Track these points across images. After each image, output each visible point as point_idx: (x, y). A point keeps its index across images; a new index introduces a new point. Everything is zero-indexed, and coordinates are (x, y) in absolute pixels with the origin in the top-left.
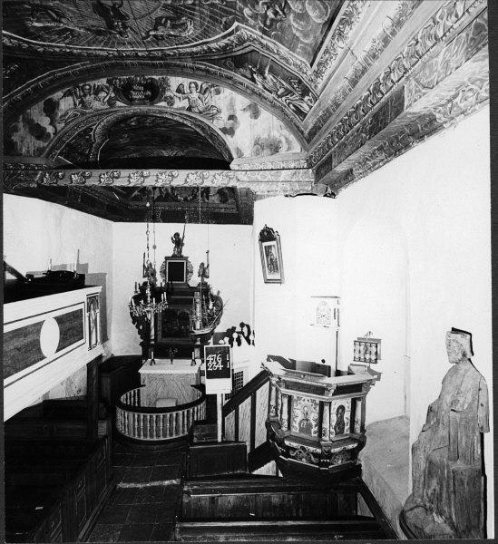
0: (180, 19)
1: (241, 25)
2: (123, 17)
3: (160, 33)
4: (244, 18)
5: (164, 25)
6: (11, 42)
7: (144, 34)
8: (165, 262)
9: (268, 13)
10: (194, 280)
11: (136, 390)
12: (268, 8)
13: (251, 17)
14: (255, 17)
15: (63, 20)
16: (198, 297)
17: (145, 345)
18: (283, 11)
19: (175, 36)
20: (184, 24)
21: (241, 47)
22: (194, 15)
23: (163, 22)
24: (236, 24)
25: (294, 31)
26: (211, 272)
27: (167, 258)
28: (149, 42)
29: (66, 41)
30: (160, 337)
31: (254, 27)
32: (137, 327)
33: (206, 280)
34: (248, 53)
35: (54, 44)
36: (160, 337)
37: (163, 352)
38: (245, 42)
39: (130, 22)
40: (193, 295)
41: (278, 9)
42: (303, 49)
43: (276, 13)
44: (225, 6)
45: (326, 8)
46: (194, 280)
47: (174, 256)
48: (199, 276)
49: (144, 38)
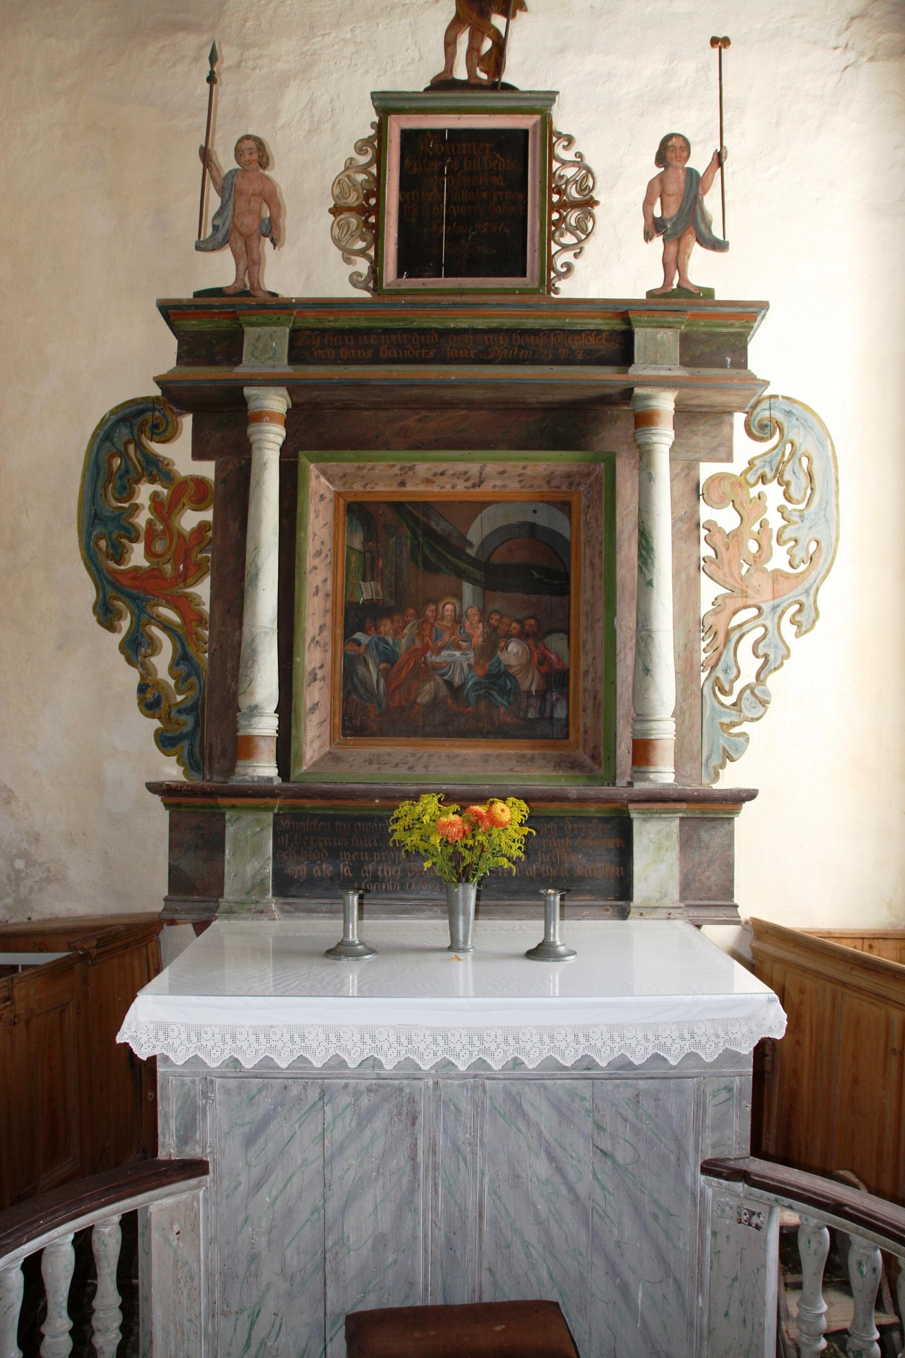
8: (381, 128)
10: (609, 263)
11: (106, 1221)
16: (656, 346)
17: (197, 815)
26: (730, 205)
27: (387, 105)
30: (314, 741)
32: (136, 648)
33: (702, 268)
36: (314, 741)
37: (341, 853)
40: (625, 357)
46: (609, 263)
47: (443, 83)
48: (654, 227)
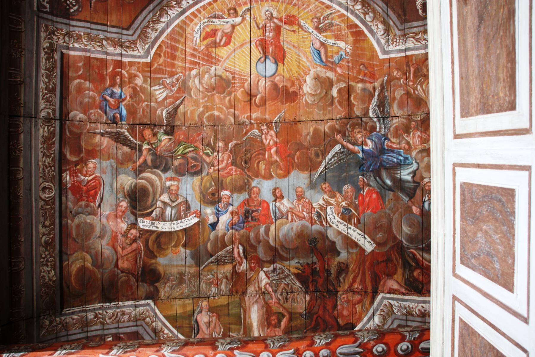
0: (207, 47)
1: (144, 60)
2: (263, 45)
3: (231, 20)
4: (143, 72)
5: (225, 34)
6: (378, 28)
7: (248, 16)
9: (120, 91)
12: (121, 96)
13: (136, 76)
14: (133, 77)
15: (317, 45)
18: (106, 100)
19: (215, 17)
20: (204, 39)
21: (142, 26)
22: (193, 56)
23: (224, 39)
24: (149, 60)
25: (91, 86)
28: (245, 3)
29: (329, 12)
31: (131, 64)
34: (137, 17)
35: (343, 11)
38: (139, 37)
39: (257, 35)
41: (111, 100)
42: (78, 69)
43: (112, 95)
44: (160, 79)
45: (70, 132)
49: (249, 10)
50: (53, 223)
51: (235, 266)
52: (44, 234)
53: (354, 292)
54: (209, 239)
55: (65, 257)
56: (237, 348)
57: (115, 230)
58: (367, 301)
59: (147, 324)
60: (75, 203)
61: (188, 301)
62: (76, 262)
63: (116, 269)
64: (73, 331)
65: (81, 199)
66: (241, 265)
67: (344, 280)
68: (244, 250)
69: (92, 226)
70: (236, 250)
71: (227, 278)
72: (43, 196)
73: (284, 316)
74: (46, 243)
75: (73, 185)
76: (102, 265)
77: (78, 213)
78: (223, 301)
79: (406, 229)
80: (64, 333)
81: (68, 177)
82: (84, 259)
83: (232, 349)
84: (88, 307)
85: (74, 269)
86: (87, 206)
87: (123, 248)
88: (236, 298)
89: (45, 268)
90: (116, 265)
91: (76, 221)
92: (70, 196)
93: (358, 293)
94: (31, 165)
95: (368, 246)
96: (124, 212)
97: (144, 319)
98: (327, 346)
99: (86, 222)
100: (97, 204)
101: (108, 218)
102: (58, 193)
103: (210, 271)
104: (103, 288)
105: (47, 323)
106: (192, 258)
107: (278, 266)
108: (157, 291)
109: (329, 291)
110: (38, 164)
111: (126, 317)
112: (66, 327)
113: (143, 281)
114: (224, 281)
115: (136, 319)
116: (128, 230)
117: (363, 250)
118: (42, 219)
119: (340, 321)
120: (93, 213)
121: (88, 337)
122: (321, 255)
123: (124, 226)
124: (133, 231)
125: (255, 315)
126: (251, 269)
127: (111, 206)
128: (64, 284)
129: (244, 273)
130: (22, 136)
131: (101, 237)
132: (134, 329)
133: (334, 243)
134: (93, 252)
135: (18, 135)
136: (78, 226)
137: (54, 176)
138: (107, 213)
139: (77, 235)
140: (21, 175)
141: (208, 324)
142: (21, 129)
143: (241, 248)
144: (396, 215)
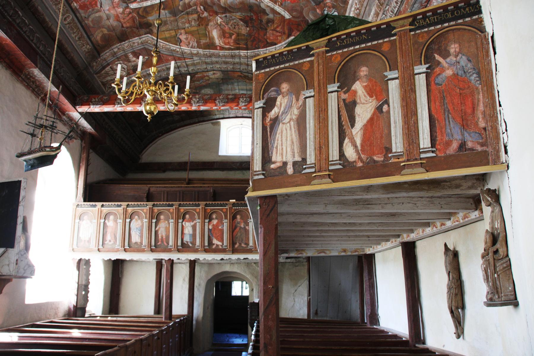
50: (78, 28)
51: (199, 15)
52: (76, 36)
53: (277, 32)
54: (179, 5)
55: (91, 37)
56: (202, 105)
57: (115, 13)
58: (284, 37)
59: (149, 43)
60: (85, 13)
61: (171, 31)
62: (98, 36)
63: (123, 29)
64: (109, 59)
65: (88, 8)
66: (203, 14)
67: (271, 25)
68: (204, 8)
69: (100, 18)
70: (199, 9)
71: (195, 20)
72: (66, 23)
73: (233, 34)
74: (79, 38)
75: (80, 6)
76: (114, 30)
77: (89, 16)
78: (195, 29)
79: (311, 16)
80: (104, 62)
81: (75, 4)
82: (102, 31)
83: (199, 106)
84: (113, 47)
85: (98, 38)
86: (93, 10)
87: (124, 19)
88: (203, 27)
89: (84, 47)
90: (123, 27)
91: (90, 19)
92: (81, 11)
93: (280, 32)
94: (52, 15)
95: (287, 16)
96: (118, 4)
97: (147, 42)
98: (245, 106)
99: (96, 17)
100: (99, 7)
101: (109, 10)
102: (73, 15)
103: (184, 18)
104: (118, 38)
105: (95, 64)
106: (170, 13)
107: (228, 15)
108: (152, 30)
109: (261, 28)
110: (55, 12)
111: (136, 44)
112: (105, 60)
113: (141, 28)
114: (193, 21)
115: (142, 43)
116: (124, 11)
117: (283, 17)
118: (71, 32)
119: (268, 41)
120: (99, 11)
121: (118, 58)
122: (256, 13)
123: (121, 10)
124: (128, 10)
125: (215, 34)
126: (210, 15)
127: (109, 4)
128: (96, 46)
129: (206, 18)
130: (39, 8)
131: (108, 19)
132: (143, 47)
133: (264, 10)
134: (106, 27)
135: (37, 10)
136: (92, 21)
137: (67, 10)
138: (108, 8)
139: (94, 25)
140: (50, 24)
141: (187, 39)
142: (37, 4)
143: (202, 7)
144: (307, 8)
